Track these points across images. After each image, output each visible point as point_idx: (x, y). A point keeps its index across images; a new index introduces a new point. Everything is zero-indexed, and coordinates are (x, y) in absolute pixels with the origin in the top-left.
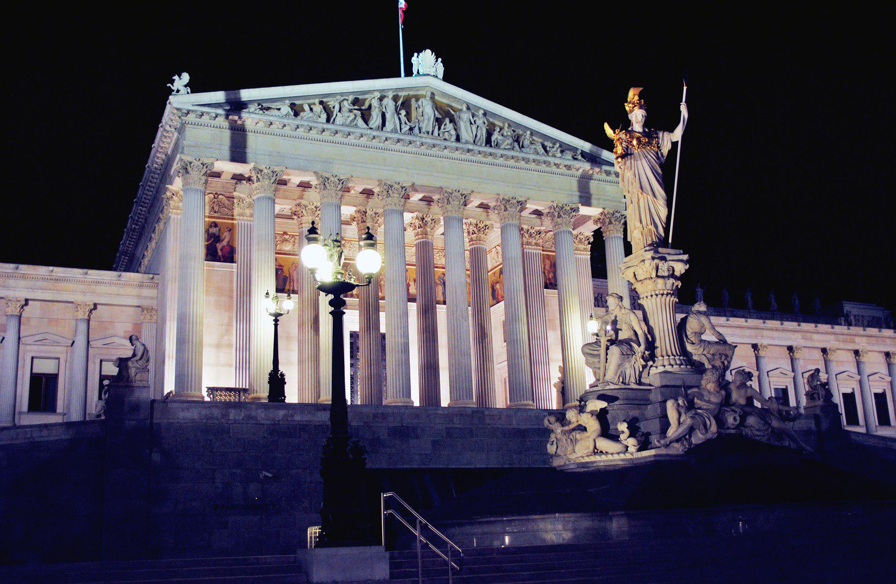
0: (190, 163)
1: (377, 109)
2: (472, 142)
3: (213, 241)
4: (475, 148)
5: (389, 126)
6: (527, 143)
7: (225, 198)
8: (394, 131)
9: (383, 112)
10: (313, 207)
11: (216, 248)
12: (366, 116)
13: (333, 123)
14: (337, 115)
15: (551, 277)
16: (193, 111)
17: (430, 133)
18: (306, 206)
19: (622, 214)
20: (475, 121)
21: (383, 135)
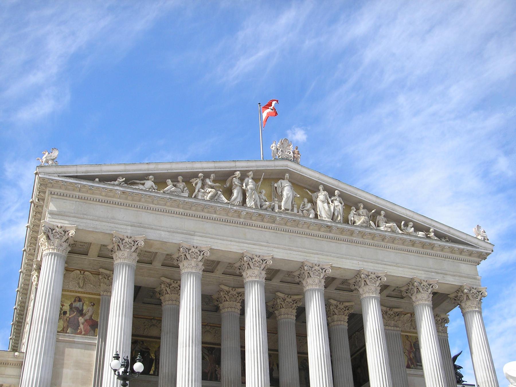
0: (53, 230)
1: (238, 188)
4: (333, 224)
5: (250, 203)
9: (243, 189)
11: (79, 322)
14: (199, 191)
15: (411, 356)
17: (290, 210)
18: (170, 285)
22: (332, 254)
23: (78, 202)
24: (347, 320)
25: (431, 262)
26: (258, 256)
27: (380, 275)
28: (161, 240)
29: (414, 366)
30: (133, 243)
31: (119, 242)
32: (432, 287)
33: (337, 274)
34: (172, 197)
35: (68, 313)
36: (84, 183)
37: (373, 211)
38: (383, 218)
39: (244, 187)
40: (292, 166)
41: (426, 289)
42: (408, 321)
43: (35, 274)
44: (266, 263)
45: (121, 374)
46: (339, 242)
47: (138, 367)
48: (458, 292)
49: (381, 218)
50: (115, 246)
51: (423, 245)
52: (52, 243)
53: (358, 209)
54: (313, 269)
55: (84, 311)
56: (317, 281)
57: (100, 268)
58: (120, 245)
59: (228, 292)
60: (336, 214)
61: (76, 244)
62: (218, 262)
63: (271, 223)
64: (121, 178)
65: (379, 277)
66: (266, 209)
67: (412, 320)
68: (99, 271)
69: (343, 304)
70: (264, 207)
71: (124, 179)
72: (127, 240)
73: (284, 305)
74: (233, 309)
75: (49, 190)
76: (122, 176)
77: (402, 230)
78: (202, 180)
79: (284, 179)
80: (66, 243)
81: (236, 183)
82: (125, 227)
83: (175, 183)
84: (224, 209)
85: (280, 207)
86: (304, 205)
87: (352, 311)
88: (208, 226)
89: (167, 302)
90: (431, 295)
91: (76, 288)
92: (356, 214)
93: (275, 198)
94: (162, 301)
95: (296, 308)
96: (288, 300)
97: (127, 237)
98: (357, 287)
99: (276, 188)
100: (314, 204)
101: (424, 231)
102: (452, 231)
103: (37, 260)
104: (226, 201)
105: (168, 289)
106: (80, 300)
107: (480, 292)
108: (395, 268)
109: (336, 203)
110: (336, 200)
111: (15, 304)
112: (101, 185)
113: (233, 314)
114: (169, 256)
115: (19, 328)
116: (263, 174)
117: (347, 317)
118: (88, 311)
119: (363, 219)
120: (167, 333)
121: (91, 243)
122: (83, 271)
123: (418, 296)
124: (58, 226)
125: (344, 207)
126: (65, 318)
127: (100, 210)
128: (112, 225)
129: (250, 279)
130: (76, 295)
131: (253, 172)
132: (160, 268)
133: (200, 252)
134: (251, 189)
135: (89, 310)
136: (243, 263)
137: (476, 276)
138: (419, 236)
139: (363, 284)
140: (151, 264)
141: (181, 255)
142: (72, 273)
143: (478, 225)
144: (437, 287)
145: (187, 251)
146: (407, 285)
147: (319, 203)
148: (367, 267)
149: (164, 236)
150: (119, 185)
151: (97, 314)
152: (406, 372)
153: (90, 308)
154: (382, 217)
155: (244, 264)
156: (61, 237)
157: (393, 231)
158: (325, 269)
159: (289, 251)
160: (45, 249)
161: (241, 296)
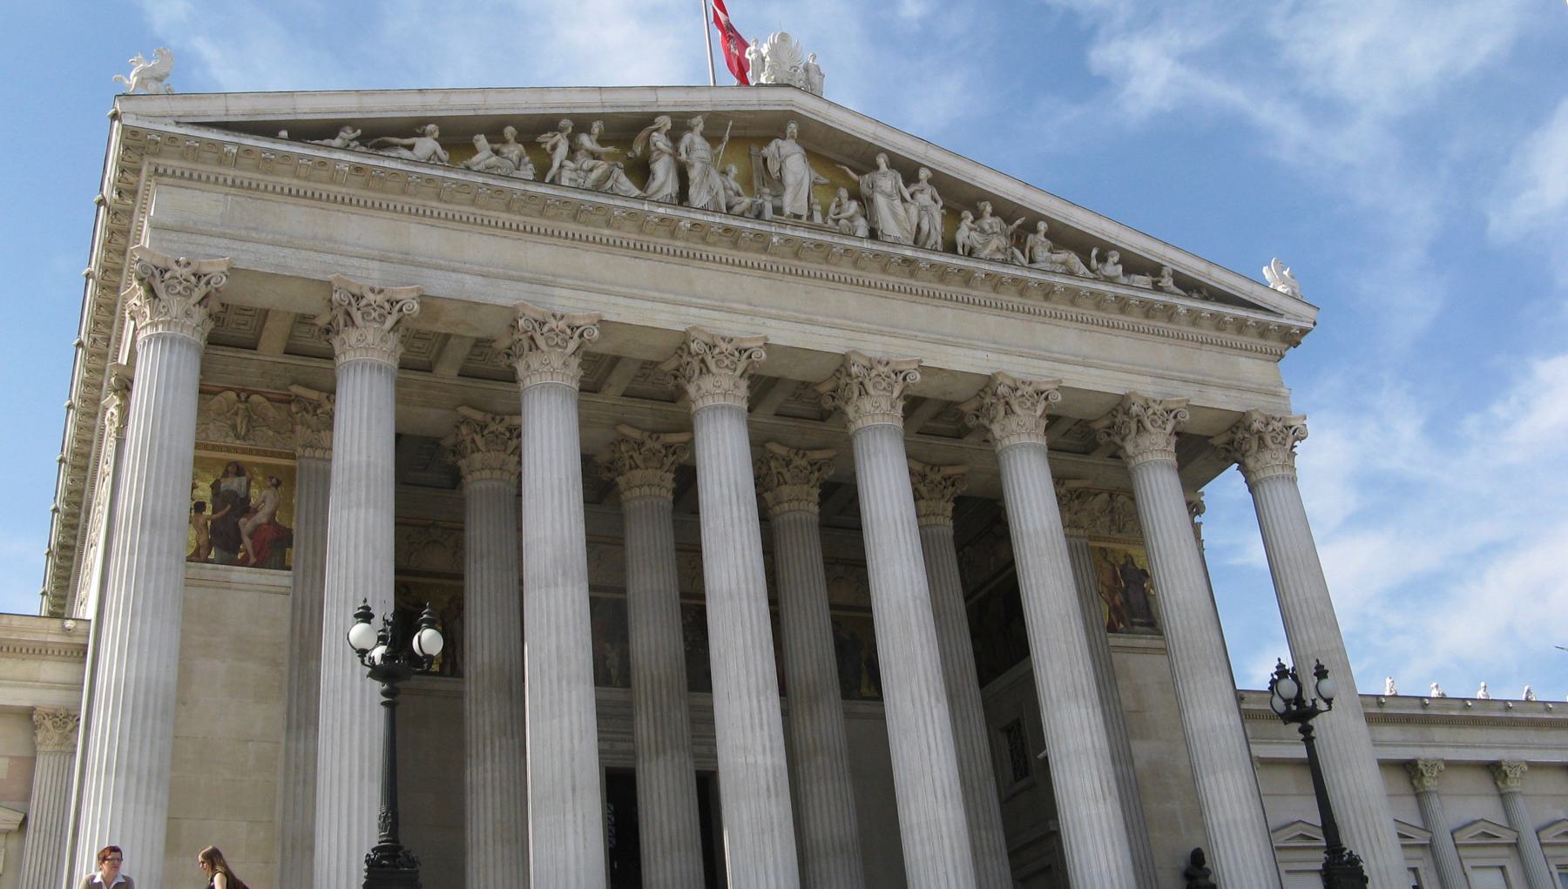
0: (163, 271)
3: (231, 510)
4: (920, 255)
5: (698, 196)
6: (1042, 253)
7: (267, 404)
8: (717, 211)
10: (501, 429)
12: (641, 172)
13: (552, 182)
14: (561, 166)
15: (1118, 603)
16: (173, 138)
17: (805, 218)
18: (484, 427)
19: (1288, 424)
20: (912, 196)
21: (685, 216)
22: (919, 334)
23: (233, 197)
24: (949, 512)
25: (1166, 354)
26: (727, 340)
27: (1043, 387)
28: (464, 297)
29: (1125, 626)
30: (387, 306)
31: (350, 304)
32: (1175, 417)
33: (932, 390)
34: (491, 181)
35: (209, 506)
36: (249, 141)
37: (1018, 222)
38: (1044, 239)
39: (684, 157)
41: (1160, 422)
42: (1105, 511)
43: (112, 403)
44: (750, 357)
45: (378, 661)
46: (936, 302)
47: (428, 640)
48: (1234, 429)
49: (1039, 242)
50: (339, 316)
51: (1148, 310)
52: (164, 307)
53: (978, 216)
54: (874, 373)
55: (253, 501)
56: (885, 405)
57: (292, 384)
58: (353, 311)
59: (641, 444)
60: (925, 227)
61: (224, 318)
62: (615, 360)
63: (757, 251)
64: (350, 131)
65: (1042, 393)
66: (742, 215)
67: (1113, 508)
68: (288, 390)
69: (939, 470)
70: (737, 209)
71: (359, 132)
72: (371, 297)
73: (787, 476)
74: (656, 490)
75: (150, 163)
76: (353, 123)
77: (1092, 271)
78: (568, 137)
79: (784, 138)
80: (202, 307)
81: (661, 145)
82: (364, 263)
83: (496, 146)
84: (632, 214)
85: (778, 210)
86: (839, 205)
87: (962, 489)
88: (591, 261)
89: (477, 475)
90: (1174, 440)
91: (229, 440)
92: (976, 230)
93: (761, 187)
94: (464, 470)
95: (818, 484)
96: (799, 462)
97: (372, 290)
98: (986, 422)
99: (765, 160)
100: (866, 204)
101: (1148, 274)
103: (118, 365)
104: (637, 192)
105: (477, 438)
106: (239, 469)
107: (1291, 427)
108: (1080, 369)
110: (922, 191)
111: (55, 498)
112: (297, 149)
113: (655, 503)
114: (482, 345)
115: (67, 564)
116: (731, 123)
117: (950, 506)
118: (264, 501)
119: (996, 242)
120: (482, 558)
121: (267, 311)
122: (244, 393)
123: (1140, 441)
124: (177, 262)
125: (943, 211)
126: (201, 521)
127: (296, 218)
128: (328, 258)
129: (709, 402)
130: (230, 458)
131: (703, 118)
132: (454, 382)
133: (572, 329)
134: (702, 160)
135: (265, 498)
136: (686, 358)
137: (1278, 389)
139: (1002, 413)
140: (431, 371)
141: (520, 340)
142: (213, 401)
144: (1188, 417)
145: (537, 329)
146: (1110, 415)
147: (881, 201)
148: (1013, 367)
149: (471, 287)
150: (345, 148)
151: (290, 509)
152: (1107, 642)
153: (269, 494)
154: (1041, 237)
155: (688, 363)
156: (189, 291)
157: (1071, 273)
158: (903, 374)
159: (807, 327)
160: (144, 324)
161: (674, 453)
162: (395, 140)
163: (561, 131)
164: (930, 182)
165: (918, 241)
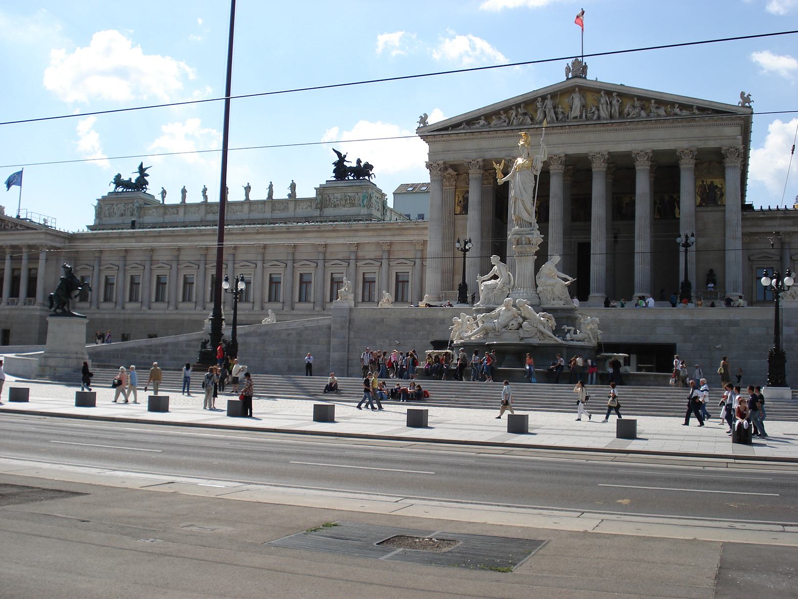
1: (541, 109)
2: (608, 118)
6: (653, 110)
8: (553, 122)
14: (514, 118)
17: (578, 117)
19: (738, 148)
35: (462, 201)
40: (579, 81)
60: (613, 112)
70: (560, 119)
72: (473, 162)
81: (538, 106)
102: (713, 104)
109: (614, 102)
127: (457, 145)
138: (682, 114)
143: (742, 92)
147: (600, 105)
154: (653, 105)
162: (475, 122)
163: (513, 109)
164: (617, 96)
165: (611, 117)
